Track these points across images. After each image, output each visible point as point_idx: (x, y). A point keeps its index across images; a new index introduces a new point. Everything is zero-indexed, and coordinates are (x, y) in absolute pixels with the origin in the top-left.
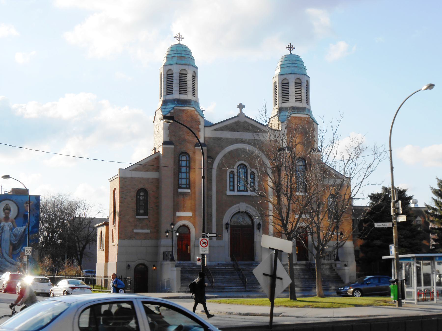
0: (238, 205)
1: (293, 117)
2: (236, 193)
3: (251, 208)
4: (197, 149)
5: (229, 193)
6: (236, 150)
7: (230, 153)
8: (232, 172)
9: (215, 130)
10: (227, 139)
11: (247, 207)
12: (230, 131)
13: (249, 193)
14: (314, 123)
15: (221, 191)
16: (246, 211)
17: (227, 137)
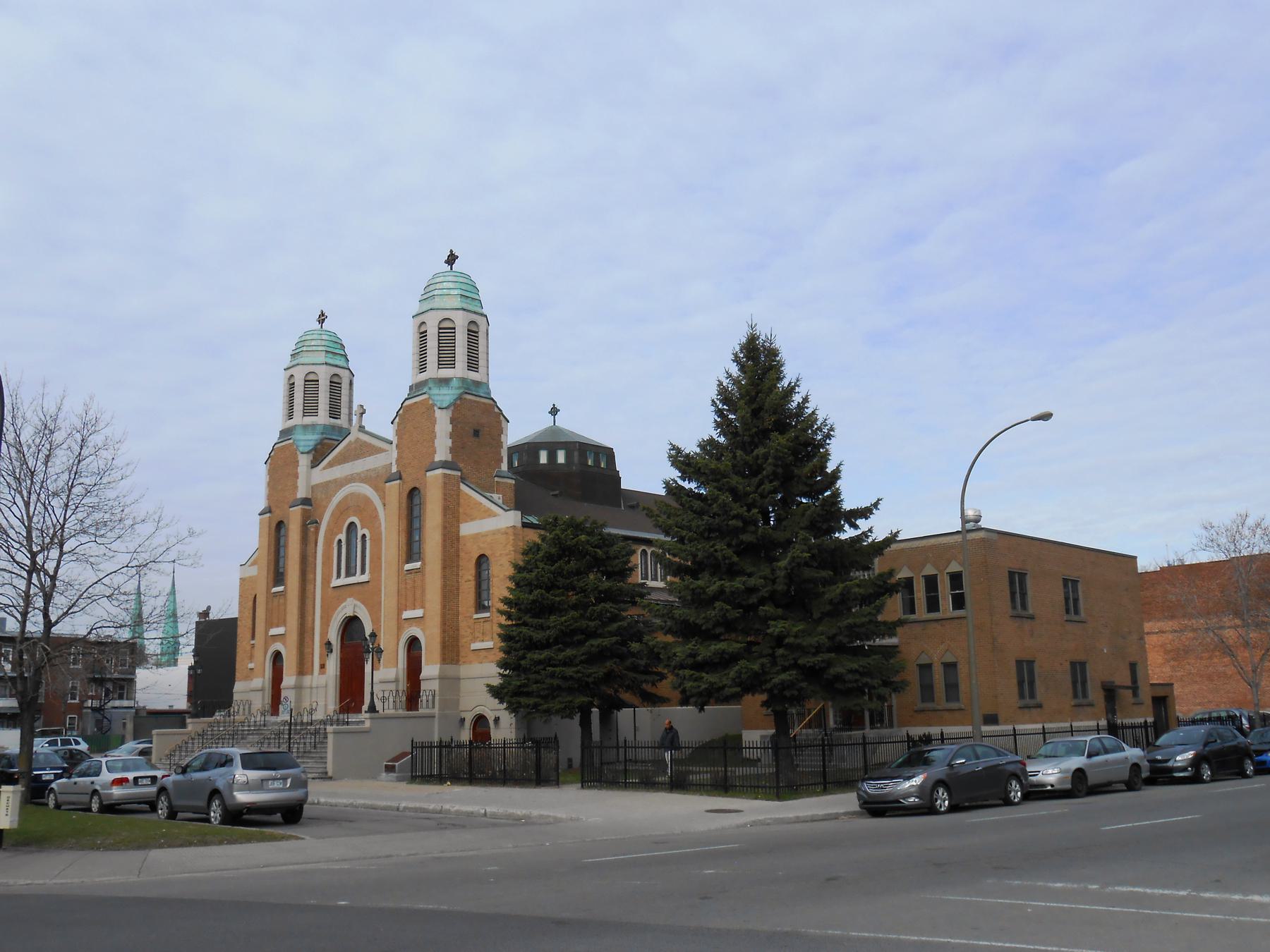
0: (344, 604)
1: (406, 406)
2: (343, 581)
6: (346, 498)
8: (340, 541)
9: (324, 468)
10: (335, 481)
13: (359, 578)
15: (326, 581)
16: (356, 614)
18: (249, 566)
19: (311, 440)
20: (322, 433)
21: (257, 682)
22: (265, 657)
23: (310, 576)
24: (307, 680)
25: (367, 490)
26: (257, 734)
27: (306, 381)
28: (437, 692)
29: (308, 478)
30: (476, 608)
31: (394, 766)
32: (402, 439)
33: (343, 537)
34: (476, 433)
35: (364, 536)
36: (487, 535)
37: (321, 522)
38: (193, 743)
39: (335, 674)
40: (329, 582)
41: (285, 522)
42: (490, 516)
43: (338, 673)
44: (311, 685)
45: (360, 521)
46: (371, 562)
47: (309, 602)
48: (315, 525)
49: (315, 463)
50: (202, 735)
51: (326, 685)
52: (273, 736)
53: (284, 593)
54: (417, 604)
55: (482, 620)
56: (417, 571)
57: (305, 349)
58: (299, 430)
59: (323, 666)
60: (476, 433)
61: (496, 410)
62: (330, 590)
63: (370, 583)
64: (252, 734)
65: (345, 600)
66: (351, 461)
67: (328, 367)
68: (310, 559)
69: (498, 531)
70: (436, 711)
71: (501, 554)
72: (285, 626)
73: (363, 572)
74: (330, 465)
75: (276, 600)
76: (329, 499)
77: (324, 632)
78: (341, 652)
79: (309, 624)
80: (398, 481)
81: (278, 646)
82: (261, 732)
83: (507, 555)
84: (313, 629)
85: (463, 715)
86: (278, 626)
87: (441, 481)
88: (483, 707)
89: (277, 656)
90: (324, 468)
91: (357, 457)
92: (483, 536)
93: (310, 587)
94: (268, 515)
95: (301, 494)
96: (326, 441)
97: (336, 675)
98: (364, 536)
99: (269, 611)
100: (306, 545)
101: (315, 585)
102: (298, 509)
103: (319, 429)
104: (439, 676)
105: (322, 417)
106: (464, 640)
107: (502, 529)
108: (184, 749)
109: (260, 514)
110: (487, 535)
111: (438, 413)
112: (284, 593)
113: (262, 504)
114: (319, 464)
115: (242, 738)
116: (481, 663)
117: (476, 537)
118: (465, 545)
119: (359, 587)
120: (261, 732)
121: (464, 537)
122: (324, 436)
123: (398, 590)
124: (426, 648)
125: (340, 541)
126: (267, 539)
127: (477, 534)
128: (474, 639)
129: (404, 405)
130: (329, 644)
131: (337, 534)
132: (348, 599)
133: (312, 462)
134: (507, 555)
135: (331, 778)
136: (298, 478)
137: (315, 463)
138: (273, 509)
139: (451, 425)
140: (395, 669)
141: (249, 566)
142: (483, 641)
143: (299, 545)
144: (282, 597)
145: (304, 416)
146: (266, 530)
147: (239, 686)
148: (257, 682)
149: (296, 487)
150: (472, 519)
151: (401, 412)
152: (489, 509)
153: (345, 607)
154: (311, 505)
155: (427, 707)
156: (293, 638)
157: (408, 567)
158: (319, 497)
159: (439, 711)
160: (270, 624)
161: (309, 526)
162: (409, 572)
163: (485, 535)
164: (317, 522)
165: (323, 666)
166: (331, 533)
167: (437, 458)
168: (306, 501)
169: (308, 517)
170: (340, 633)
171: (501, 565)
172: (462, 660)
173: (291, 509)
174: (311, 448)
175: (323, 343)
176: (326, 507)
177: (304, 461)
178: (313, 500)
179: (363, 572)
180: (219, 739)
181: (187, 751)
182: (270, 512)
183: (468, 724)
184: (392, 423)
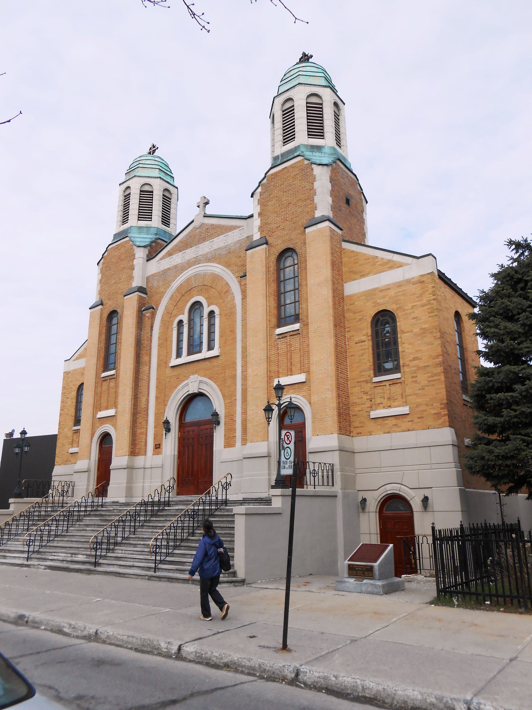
1: (272, 175)
2: (185, 359)
3: (206, 383)
4: (126, 299)
5: (175, 362)
6: (188, 280)
7: (178, 289)
8: (181, 322)
9: (161, 259)
10: (176, 267)
11: (201, 382)
12: (180, 251)
13: (205, 354)
14: (313, 166)
15: (163, 362)
16: (201, 391)
17: (176, 264)
18: (74, 360)
19: (146, 238)
20: (156, 234)
21: (82, 464)
22: (92, 439)
23: (145, 358)
24: (139, 461)
25: (217, 269)
26: (96, 515)
27: (141, 191)
28: (337, 467)
29: (144, 269)
30: (374, 370)
31: (371, 568)
32: (266, 206)
33: (185, 317)
34: (348, 202)
35: (211, 313)
36: (389, 289)
37: (157, 308)
38: (17, 525)
39: (173, 453)
40: (166, 363)
41: (119, 311)
42: (391, 268)
43: (176, 453)
44: (144, 465)
45: (206, 298)
46: (221, 336)
47: (143, 384)
48: (151, 310)
49: (150, 258)
50: (28, 516)
51: (162, 465)
52: (129, 518)
53: (115, 376)
54: (294, 369)
55: (387, 384)
56: (296, 333)
57: (140, 165)
58: (134, 230)
59: (158, 447)
60: (348, 202)
61: (359, 188)
62: (168, 371)
63: (220, 358)
64: (89, 515)
65: (187, 377)
66: (196, 245)
67: (162, 181)
68: (145, 343)
69: (408, 281)
70: (337, 488)
71: (413, 307)
72: (116, 407)
73: (210, 348)
74: (170, 254)
75: (105, 384)
76: (168, 285)
77: (159, 413)
78: (180, 431)
79: (143, 404)
80: (265, 246)
81: (108, 428)
82: (98, 513)
83: (423, 306)
84: (147, 409)
85: (365, 495)
86: (107, 408)
87: (328, 233)
88: (399, 485)
89: (106, 438)
90: (161, 259)
91: (203, 239)
92: (381, 291)
93: (144, 369)
94: (100, 307)
95: (137, 282)
96: (159, 241)
97: (174, 455)
98: (211, 313)
99: (98, 396)
100: (141, 329)
101: (150, 367)
102: (134, 299)
103: (154, 231)
104: (339, 447)
105: (156, 221)
106: (357, 409)
107: (413, 278)
108: (6, 531)
109: (90, 309)
110: (389, 289)
111: (317, 170)
112: (115, 376)
113: (94, 299)
114: (154, 257)
115: (78, 520)
116: (389, 433)
117: (370, 294)
118: (354, 304)
119: (207, 363)
120: (98, 513)
121: (348, 296)
122: (158, 236)
123: (267, 356)
124: (314, 417)
125: (181, 322)
126: (98, 328)
127: (374, 290)
128: (377, 406)
129: (268, 174)
130: (167, 423)
131: (176, 316)
132: (192, 377)
133: (147, 256)
134: (423, 306)
135: (243, 582)
136: (133, 269)
137: (150, 258)
138: (104, 302)
139: (330, 184)
140: (266, 442)
141: (74, 360)
142: (390, 406)
143: (134, 329)
144: (113, 380)
145: (139, 220)
146: (97, 321)
147: (57, 470)
148: (82, 464)
149: (131, 278)
150: (363, 276)
151: (265, 181)
152: (389, 261)
153: (187, 384)
154: (146, 294)
155: (323, 485)
156: (125, 419)
157: (279, 331)
158: (155, 285)
159: (342, 489)
160: (97, 407)
161: (144, 312)
162: (281, 337)
163: (388, 288)
164: (153, 308)
165: (158, 447)
166: (169, 314)
167: (318, 214)
168: (141, 290)
169: (144, 304)
170: (179, 412)
171: (413, 318)
172: (355, 431)
173: (126, 297)
174: (147, 243)
175: (157, 163)
176: (163, 293)
177: (141, 254)
178: (148, 290)
179: (210, 348)
180: (52, 520)
181: (9, 534)
182: (102, 304)
183: (373, 505)
184: (252, 196)
